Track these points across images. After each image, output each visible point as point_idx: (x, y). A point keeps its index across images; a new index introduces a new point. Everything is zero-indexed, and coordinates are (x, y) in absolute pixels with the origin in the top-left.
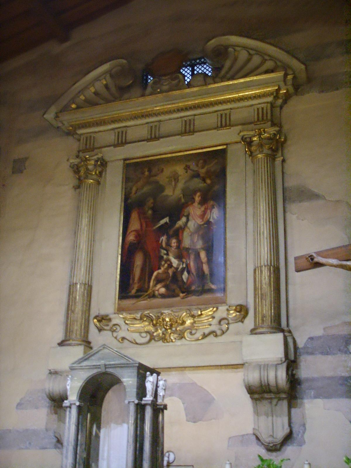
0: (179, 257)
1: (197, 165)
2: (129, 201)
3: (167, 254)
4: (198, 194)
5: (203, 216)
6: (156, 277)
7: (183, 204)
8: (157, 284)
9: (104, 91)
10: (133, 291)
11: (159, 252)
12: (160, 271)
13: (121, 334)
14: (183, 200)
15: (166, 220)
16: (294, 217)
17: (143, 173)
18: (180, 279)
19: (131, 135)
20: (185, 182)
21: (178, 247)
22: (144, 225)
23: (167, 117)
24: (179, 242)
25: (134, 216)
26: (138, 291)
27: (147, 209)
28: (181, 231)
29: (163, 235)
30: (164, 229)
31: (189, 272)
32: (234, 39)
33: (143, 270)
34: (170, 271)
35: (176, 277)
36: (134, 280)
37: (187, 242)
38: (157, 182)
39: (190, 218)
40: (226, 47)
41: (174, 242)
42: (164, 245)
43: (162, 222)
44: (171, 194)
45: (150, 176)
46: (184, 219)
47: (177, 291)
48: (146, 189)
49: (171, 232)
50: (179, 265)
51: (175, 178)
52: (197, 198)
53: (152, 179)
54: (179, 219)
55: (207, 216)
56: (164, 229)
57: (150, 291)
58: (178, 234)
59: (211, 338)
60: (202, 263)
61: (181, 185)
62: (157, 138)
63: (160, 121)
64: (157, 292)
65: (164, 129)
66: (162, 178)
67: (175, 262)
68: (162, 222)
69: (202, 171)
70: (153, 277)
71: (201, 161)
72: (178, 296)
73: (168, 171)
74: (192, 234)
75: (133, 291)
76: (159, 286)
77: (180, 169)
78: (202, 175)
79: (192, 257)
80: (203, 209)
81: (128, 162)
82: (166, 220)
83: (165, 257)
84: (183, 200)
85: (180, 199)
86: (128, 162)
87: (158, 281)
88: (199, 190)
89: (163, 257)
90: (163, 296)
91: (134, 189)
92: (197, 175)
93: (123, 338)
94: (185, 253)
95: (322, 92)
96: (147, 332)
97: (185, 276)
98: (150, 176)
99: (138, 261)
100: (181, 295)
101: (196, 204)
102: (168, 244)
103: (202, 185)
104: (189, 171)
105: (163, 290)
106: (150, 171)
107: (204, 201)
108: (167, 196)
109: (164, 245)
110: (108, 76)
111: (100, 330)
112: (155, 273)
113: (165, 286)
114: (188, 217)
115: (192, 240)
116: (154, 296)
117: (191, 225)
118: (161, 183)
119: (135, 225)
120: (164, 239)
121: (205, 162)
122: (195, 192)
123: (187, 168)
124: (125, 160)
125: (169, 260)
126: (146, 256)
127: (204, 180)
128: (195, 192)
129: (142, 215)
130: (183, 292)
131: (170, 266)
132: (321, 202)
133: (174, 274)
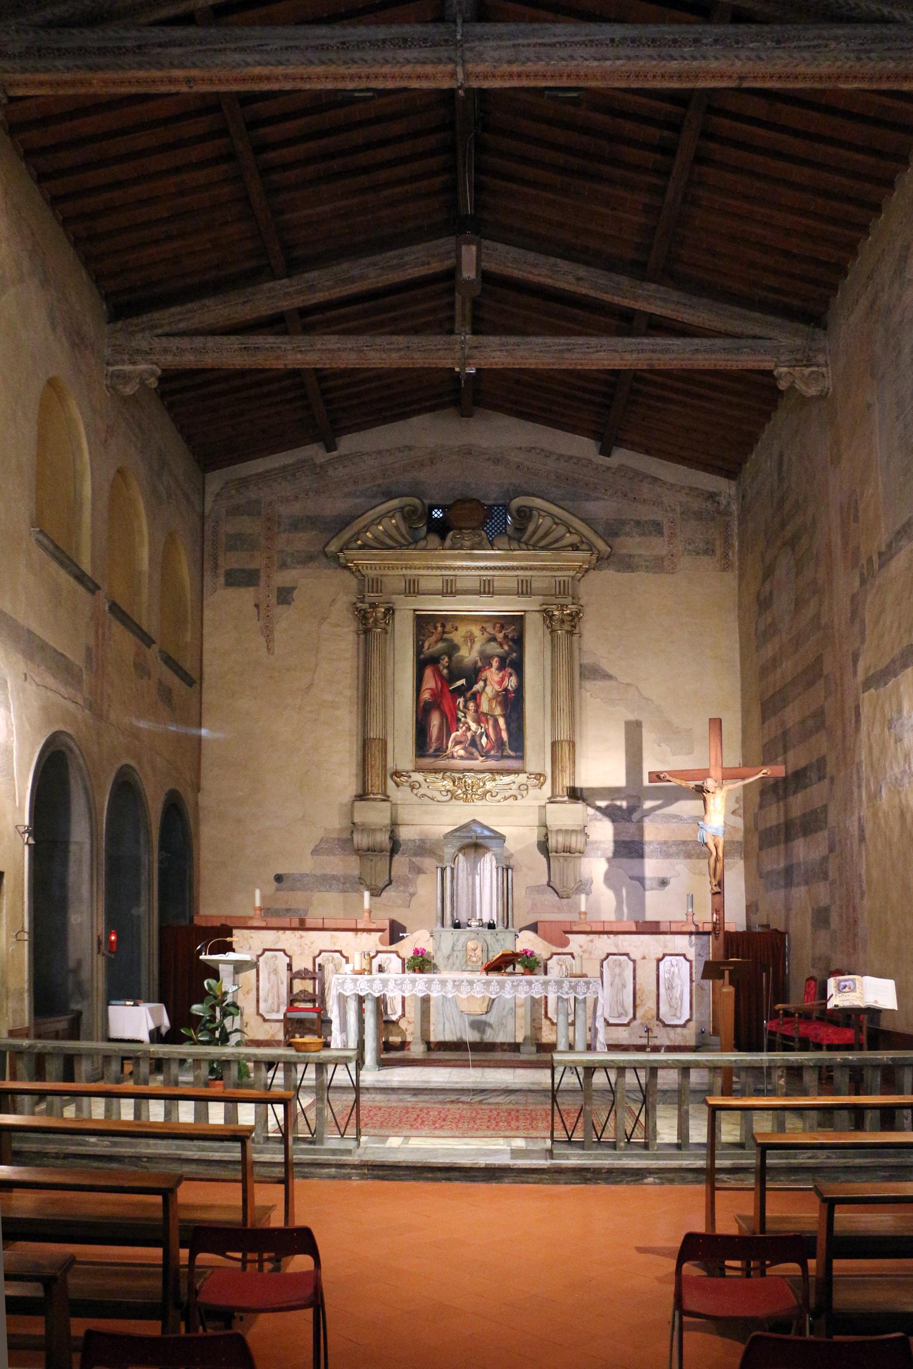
0: (478, 722)
1: (494, 628)
2: (422, 656)
3: (465, 717)
4: (496, 659)
5: (500, 683)
6: (454, 739)
7: (480, 668)
8: (455, 745)
9: (394, 533)
10: (431, 750)
11: (457, 714)
12: (458, 733)
13: (422, 791)
14: (480, 664)
15: (462, 681)
16: (588, 694)
17: (436, 628)
18: (478, 743)
19: (424, 584)
20: (482, 645)
21: (476, 711)
22: (439, 685)
23: (465, 573)
24: (478, 706)
25: (428, 672)
26: (436, 750)
27: (441, 668)
28: (478, 697)
29: (460, 697)
30: (460, 691)
31: (487, 737)
32: (538, 502)
33: (441, 729)
34: (469, 734)
35: (474, 743)
36: (431, 739)
37: (485, 707)
38: (451, 641)
39: (488, 683)
40: (531, 509)
41: (471, 705)
42: (461, 707)
43: (459, 683)
44: (467, 655)
45: (444, 632)
46: (481, 683)
47: (476, 754)
48: (440, 645)
49: (468, 695)
50: (477, 729)
51: (471, 638)
52: (495, 663)
53: (446, 636)
54: (476, 683)
55: (505, 683)
56: (460, 691)
57: (448, 751)
58: (475, 697)
59: (511, 801)
60: (500, 730)
61: (477, 647)
62: (453, 593)
63: (456, 576)
64: (455, 754)
65: (460, 585)
66: (457, 637)
67: (473, 726)
68: (459, 683)
69: (500, 636)
70: (451, 739)
71: (498, 625)
72: (477, 759)
73: (463, 630)
74: (490, 700)
75: (431, 750)
76: (457, 748)
77: (476, 630)
78: (499, 640)
79: (491, 722)
80: (501, 675)
81: (417, 613)
82: (462, 681)
83: (463, 719)
84: (480, 664)
85: (476, 663)
86: (417, 613)
87: (457, 743)
88: (498, 656)
89: (460, 720)
90: (462, 758)
91: (426, 645)
92: (493, 639)
93: (423, 795)
94: (483, 718)
95: (619, 571)
96: (448, 791)
97: (484, 740)
98: (444, 632)
99: (435, 721)
100: (481, 758)
101: (493, 669)
102: (465, 707)
103: (499, 651)
104: (486, 634)
105: (462, 752)
106: (443, 626)
107: (501, 668)
108: (462, 658)
109: (461, 707)
110: (398, 515)
111: (398, 785)
112: (453, 735)
113: (464, 749)
114: (485, 681)
115: (490, 706)
116: (453, 757)
117: (488, 689)
118: (456, 642)
119: (430, 682)
120: (461, 700)
121: (502, 627)
122: (491, 657)
123: (483, 629)
124: (415, 610)
125: (466, 723)
126: (443, 715)
127: (501, 645)
128: (491, 657)
129: (438, 673)
130: (482, 756)
131: (469, 729)
132: (613, 683)
133: (473, 737)
